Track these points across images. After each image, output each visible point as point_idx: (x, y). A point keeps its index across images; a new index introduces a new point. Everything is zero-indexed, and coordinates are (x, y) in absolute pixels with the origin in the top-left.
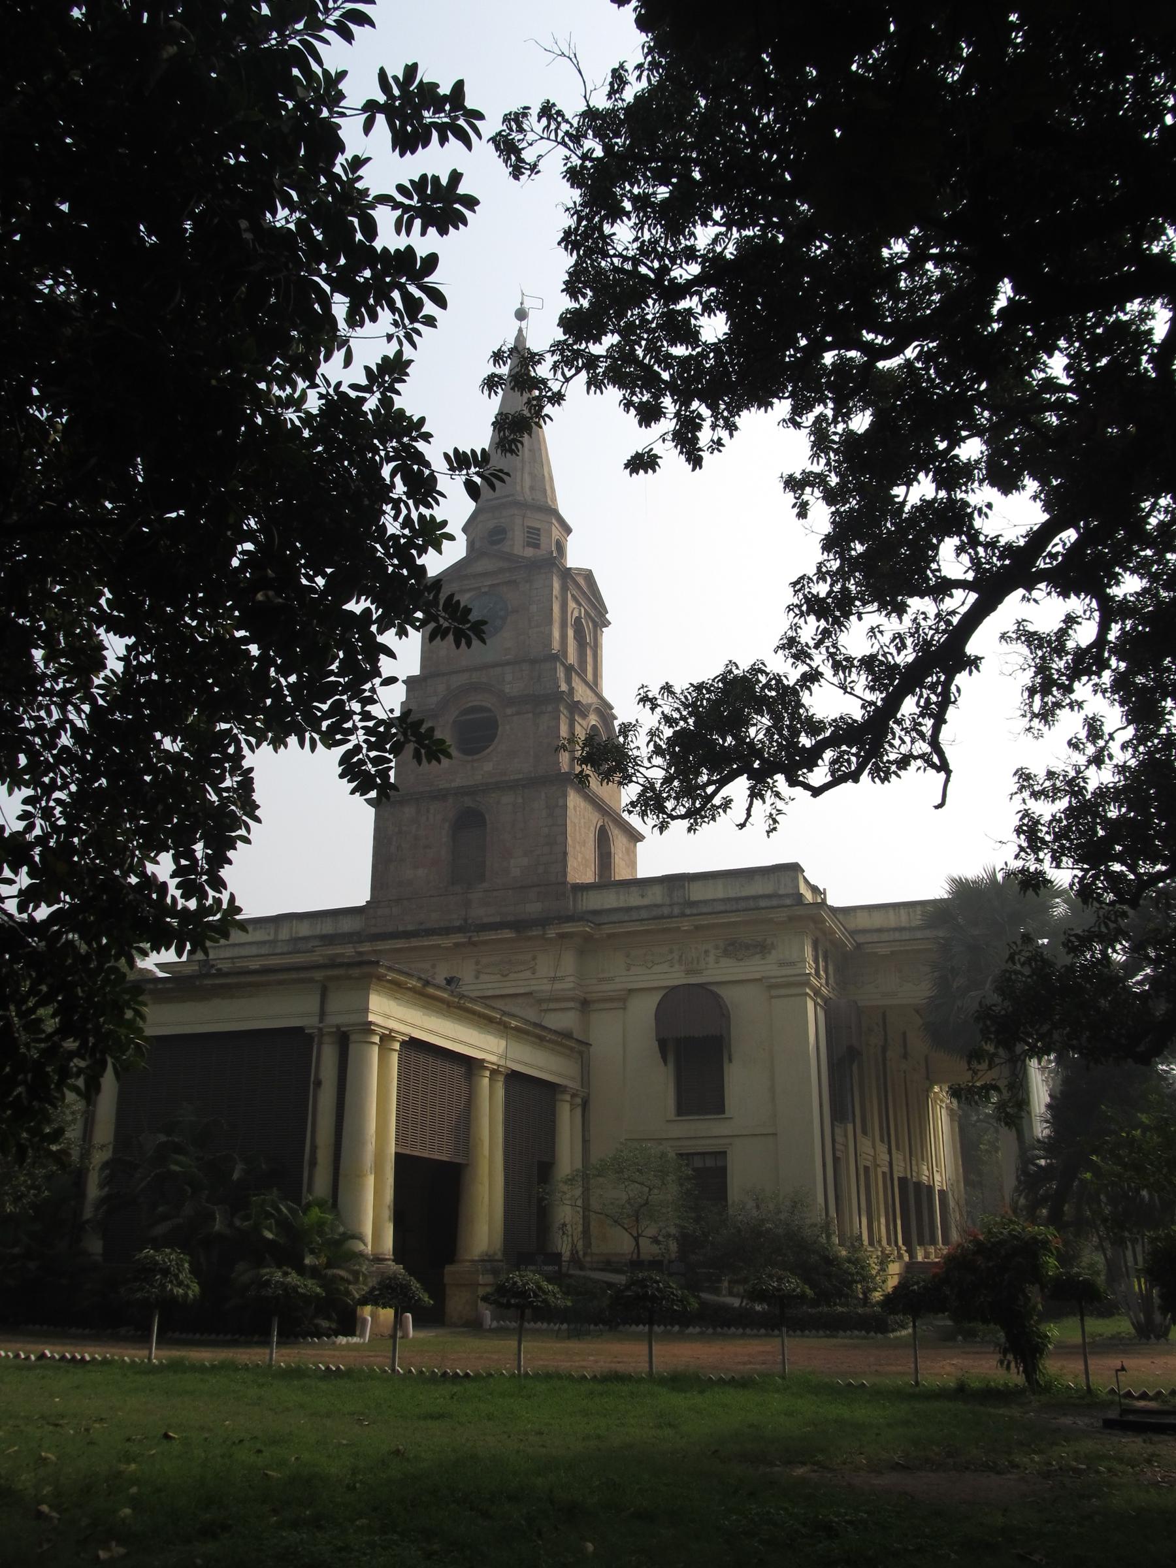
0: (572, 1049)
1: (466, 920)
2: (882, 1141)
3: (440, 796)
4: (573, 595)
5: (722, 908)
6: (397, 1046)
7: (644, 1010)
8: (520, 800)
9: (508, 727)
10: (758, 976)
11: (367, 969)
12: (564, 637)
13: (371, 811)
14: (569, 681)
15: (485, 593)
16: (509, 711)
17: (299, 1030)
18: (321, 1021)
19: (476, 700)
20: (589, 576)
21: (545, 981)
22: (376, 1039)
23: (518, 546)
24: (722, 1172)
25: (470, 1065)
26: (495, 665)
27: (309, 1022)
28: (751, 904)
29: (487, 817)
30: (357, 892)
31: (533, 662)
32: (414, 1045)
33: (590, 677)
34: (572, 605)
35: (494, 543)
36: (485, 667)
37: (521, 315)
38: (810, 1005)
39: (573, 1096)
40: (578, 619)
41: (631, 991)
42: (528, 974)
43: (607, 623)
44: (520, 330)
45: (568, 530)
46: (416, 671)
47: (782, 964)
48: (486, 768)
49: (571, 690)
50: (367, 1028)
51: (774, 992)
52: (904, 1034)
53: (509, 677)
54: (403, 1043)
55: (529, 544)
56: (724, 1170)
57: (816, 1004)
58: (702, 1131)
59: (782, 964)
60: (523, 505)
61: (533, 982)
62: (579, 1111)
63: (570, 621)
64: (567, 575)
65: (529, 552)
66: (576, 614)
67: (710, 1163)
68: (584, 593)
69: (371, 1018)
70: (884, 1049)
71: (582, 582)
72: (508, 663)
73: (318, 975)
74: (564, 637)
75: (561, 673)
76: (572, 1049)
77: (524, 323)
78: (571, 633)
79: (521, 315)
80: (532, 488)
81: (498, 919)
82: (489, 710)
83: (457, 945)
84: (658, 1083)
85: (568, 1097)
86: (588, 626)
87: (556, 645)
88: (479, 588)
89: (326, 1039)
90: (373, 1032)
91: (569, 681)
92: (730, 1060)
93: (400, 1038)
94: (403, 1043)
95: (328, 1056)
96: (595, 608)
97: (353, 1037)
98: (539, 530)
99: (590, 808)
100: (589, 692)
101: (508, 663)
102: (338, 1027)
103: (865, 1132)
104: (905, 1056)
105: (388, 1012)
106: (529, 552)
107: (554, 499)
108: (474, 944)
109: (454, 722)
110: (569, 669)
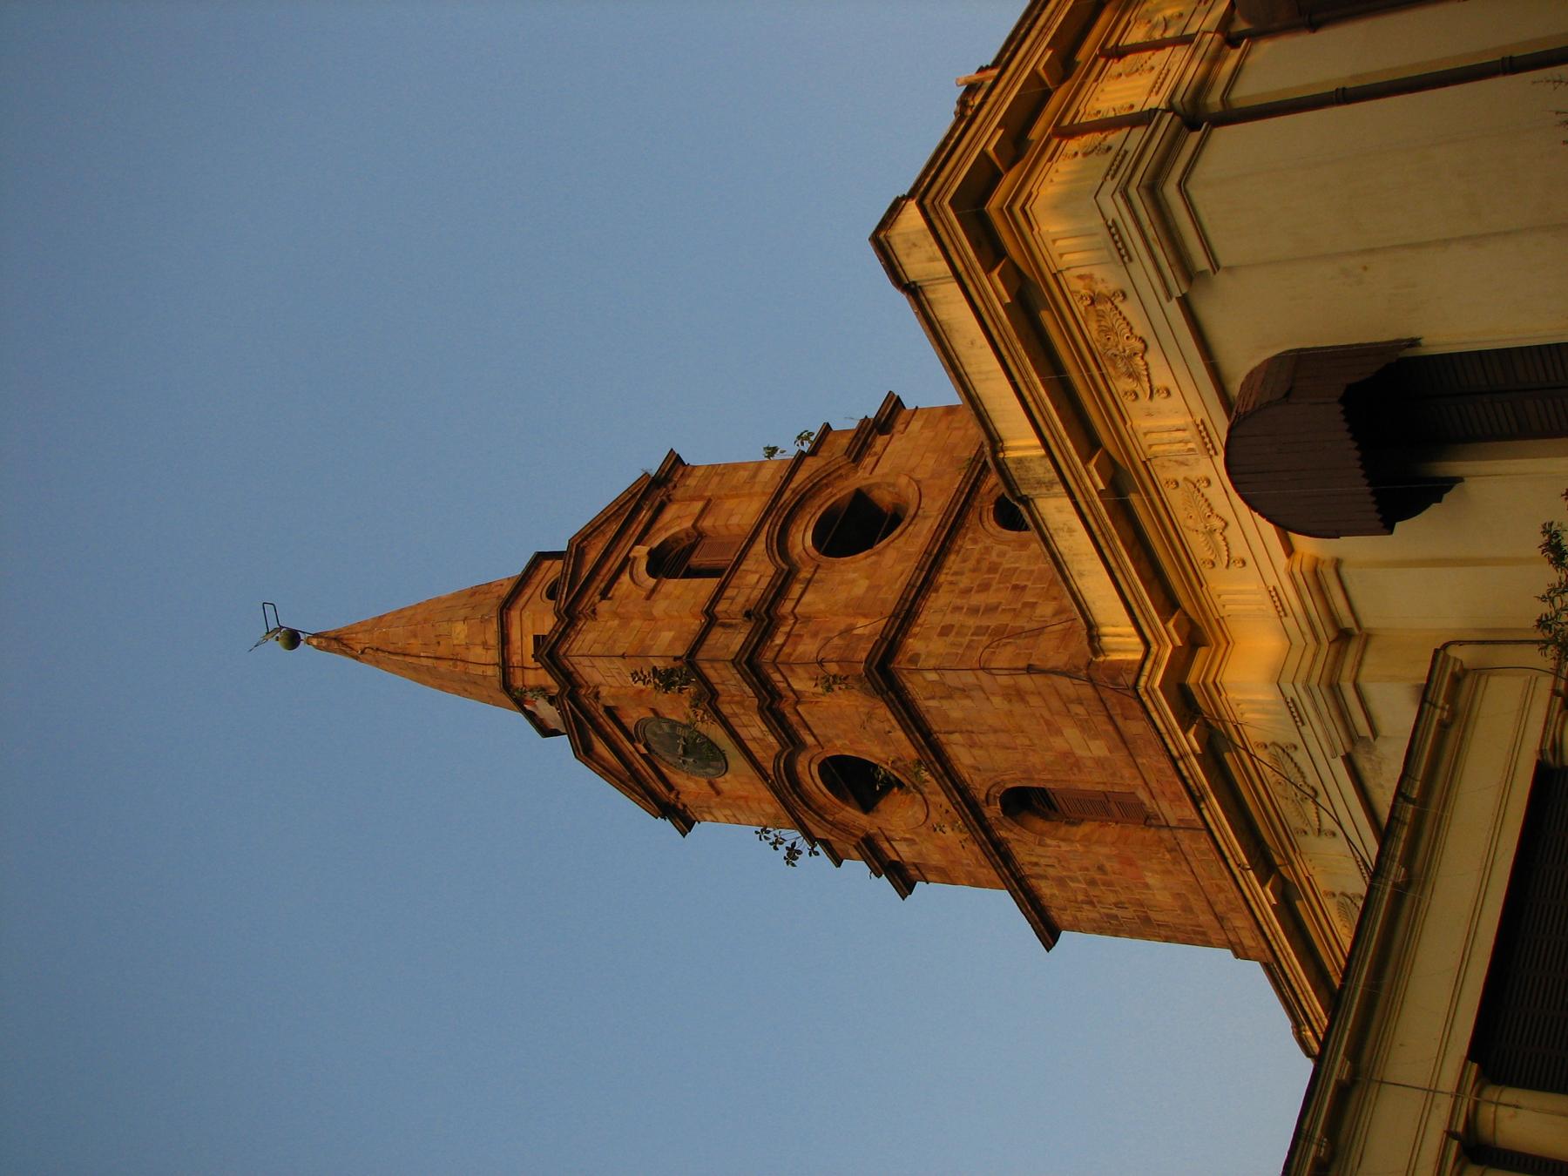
4: (604, 595)
8: (956, 737)
9: (839, 743)
10: (1173, 308)
13: (1065, 936)
15: (646, 746)
16: (810, 740)
21: (1306, 730)
29: (1010, 786)
37: (293, 639)
42: (1300, 757)
43: (674, 462)
51: (1202, 263)
53: (755, 732)
61: (1315, 750)
68: (606, 554)
71: (592, 556)
79: (293, 639)
80: (485, 645)
88: (643, 756)
92: (1414, 343)
98: (536, 638)
99: (953, 562)
110: (711, 619)
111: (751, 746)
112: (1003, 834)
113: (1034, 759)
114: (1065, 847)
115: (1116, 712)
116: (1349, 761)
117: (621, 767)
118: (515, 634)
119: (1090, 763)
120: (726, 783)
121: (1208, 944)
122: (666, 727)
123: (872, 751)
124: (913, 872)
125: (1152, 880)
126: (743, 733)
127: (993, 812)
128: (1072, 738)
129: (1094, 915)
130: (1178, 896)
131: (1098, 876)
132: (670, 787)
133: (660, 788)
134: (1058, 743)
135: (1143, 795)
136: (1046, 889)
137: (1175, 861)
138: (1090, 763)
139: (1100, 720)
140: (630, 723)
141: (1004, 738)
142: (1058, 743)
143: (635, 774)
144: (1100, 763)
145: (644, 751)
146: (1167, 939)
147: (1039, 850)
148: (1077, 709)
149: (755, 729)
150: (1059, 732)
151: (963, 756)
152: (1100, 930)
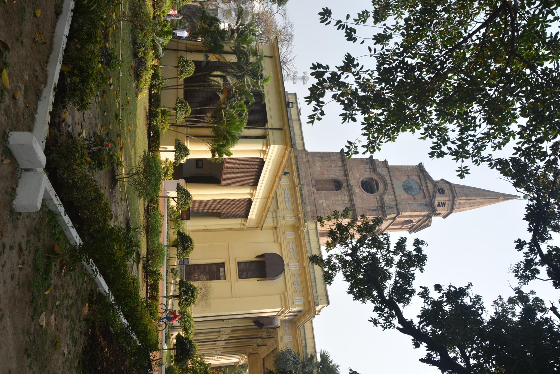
0: (260, 223)
1: (303, 185)
2: (229, 337)
3: (346, 174)
5: (312, 277)
6: (262, 157)
7: (274, 249)
8: (346, 202)
11: (289, 144)
12: (406, 216)
13: (339, 151)
14: (390, 219)
16: (378, 197)
17: (266, 121)
18: (270, 129)
19: (381, 185)
20: (428, 225)
22: (264, 149)
23: (439, 198)
24: (218, 278)
25: (255, 184)
26: (394, 191)
27: (269, 125)
28: (314, 287)
30: (310, 147)
31: (396, 205)
32: (261, 163)
33: (391, 227)
34: (417, 219)
35: (438, 190)
36: (393, 188)
38: (278, 310)
39: (243, 224)
40: (412, 222)
41: (281, 244)
42: (285, 207)
44: (520, 197)
45: (444, 217)
46: (390, 164)
47: (292, 299)
48: (358, 190)
49: (387, 220)
50: (268, 145)
51: (282, 296)
52: (266, 345)
53: (390, 197)
54: (263, 159)
55: (439, 203)
56: (220, 279)
57: (278, 312)
58: (232, 270)
59: (292, 299)
60: (453, 200)
62: (239, 226)
63: (412, 219)
64: (429, 217)
65: (436, 203)
66: (414, 221)
67: (222, 274)
68: (422, 224)
69: (272, 146)
70: (261, 338)
71: (426, 223)
72: (395, 196)
73: (286, 127)
74: (406, 216)
75: (393, 216)
76: (260, 223)
77: (522, 198)
78: (407, 219)
80: (460, 203)
81: (304, 196)
82: (378, 190)
83: (294, 182)
84: (249, 254)
85: (243, 223)
86: (409, 226)
87: (404, 214)
89: (263, 131)
90: (267, 147)
91: (390, 219)
93: (265, 158)
94: (263, 159)
95: (257, 132)
96: (416, 228)
97: (264, 140)
100: (386, 226)
101: (395, 196)
102: (268, 135)
103: (233, 331)
104: (258, 346)
105: (273, 153)
106: (436, 203)
107: (456, 212)
108: (295, 188)
109: (373, 178)
110: (394, 219)
111: (392, 193)
112: (345, 178)
113: (333, 198)
114: (333, 176)
115: (315, 212)
116: (278, 208)
117: (428, 181)
118: (450, 207)
119: (323, 198)
120: (405, 178)
121: (312, 153)
122: (413, 193)
123: (365, 195)
124: (368, 161)
125: (319, 168)
126: (393, 196)
127: (345, 184)
128: (325, 205)
129: (332, 157)
130: (315, 165)
131: (329, 169)
132: (419, 176)
133: (422, 176)
134: (328, 202)
135: (315, 191)
136: (340, 163)
137: (313, 174)
138: (323, 198)
139: (319, 209)
140: (422, 194)
141: (337, 203)
142: (328, 202)
143: (425, 180)
144: (321, 199)
145: (421, 187)
146: (320, 152)
147: (338, 174)
148: (322, 211)
149: (388, 199)
150: (327, 205)
151: (346, 198)
152: (333, 153)
